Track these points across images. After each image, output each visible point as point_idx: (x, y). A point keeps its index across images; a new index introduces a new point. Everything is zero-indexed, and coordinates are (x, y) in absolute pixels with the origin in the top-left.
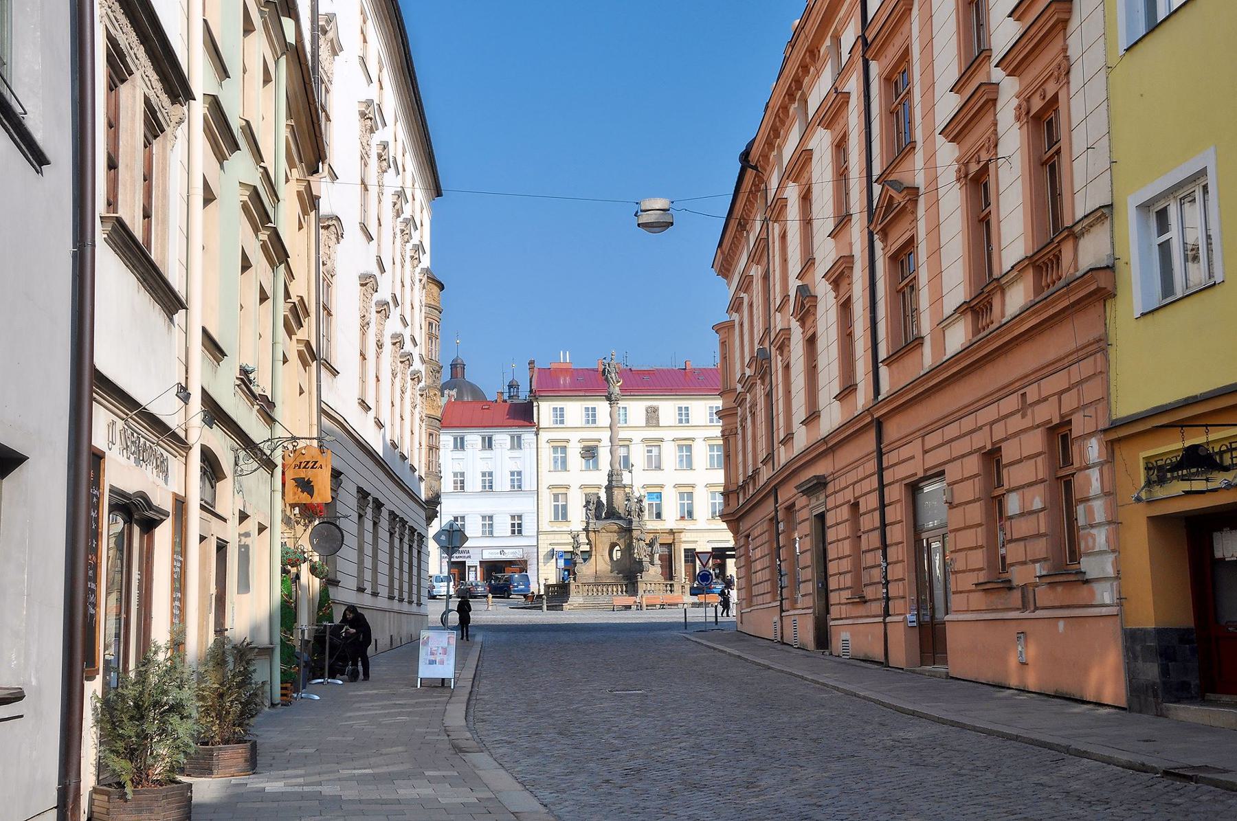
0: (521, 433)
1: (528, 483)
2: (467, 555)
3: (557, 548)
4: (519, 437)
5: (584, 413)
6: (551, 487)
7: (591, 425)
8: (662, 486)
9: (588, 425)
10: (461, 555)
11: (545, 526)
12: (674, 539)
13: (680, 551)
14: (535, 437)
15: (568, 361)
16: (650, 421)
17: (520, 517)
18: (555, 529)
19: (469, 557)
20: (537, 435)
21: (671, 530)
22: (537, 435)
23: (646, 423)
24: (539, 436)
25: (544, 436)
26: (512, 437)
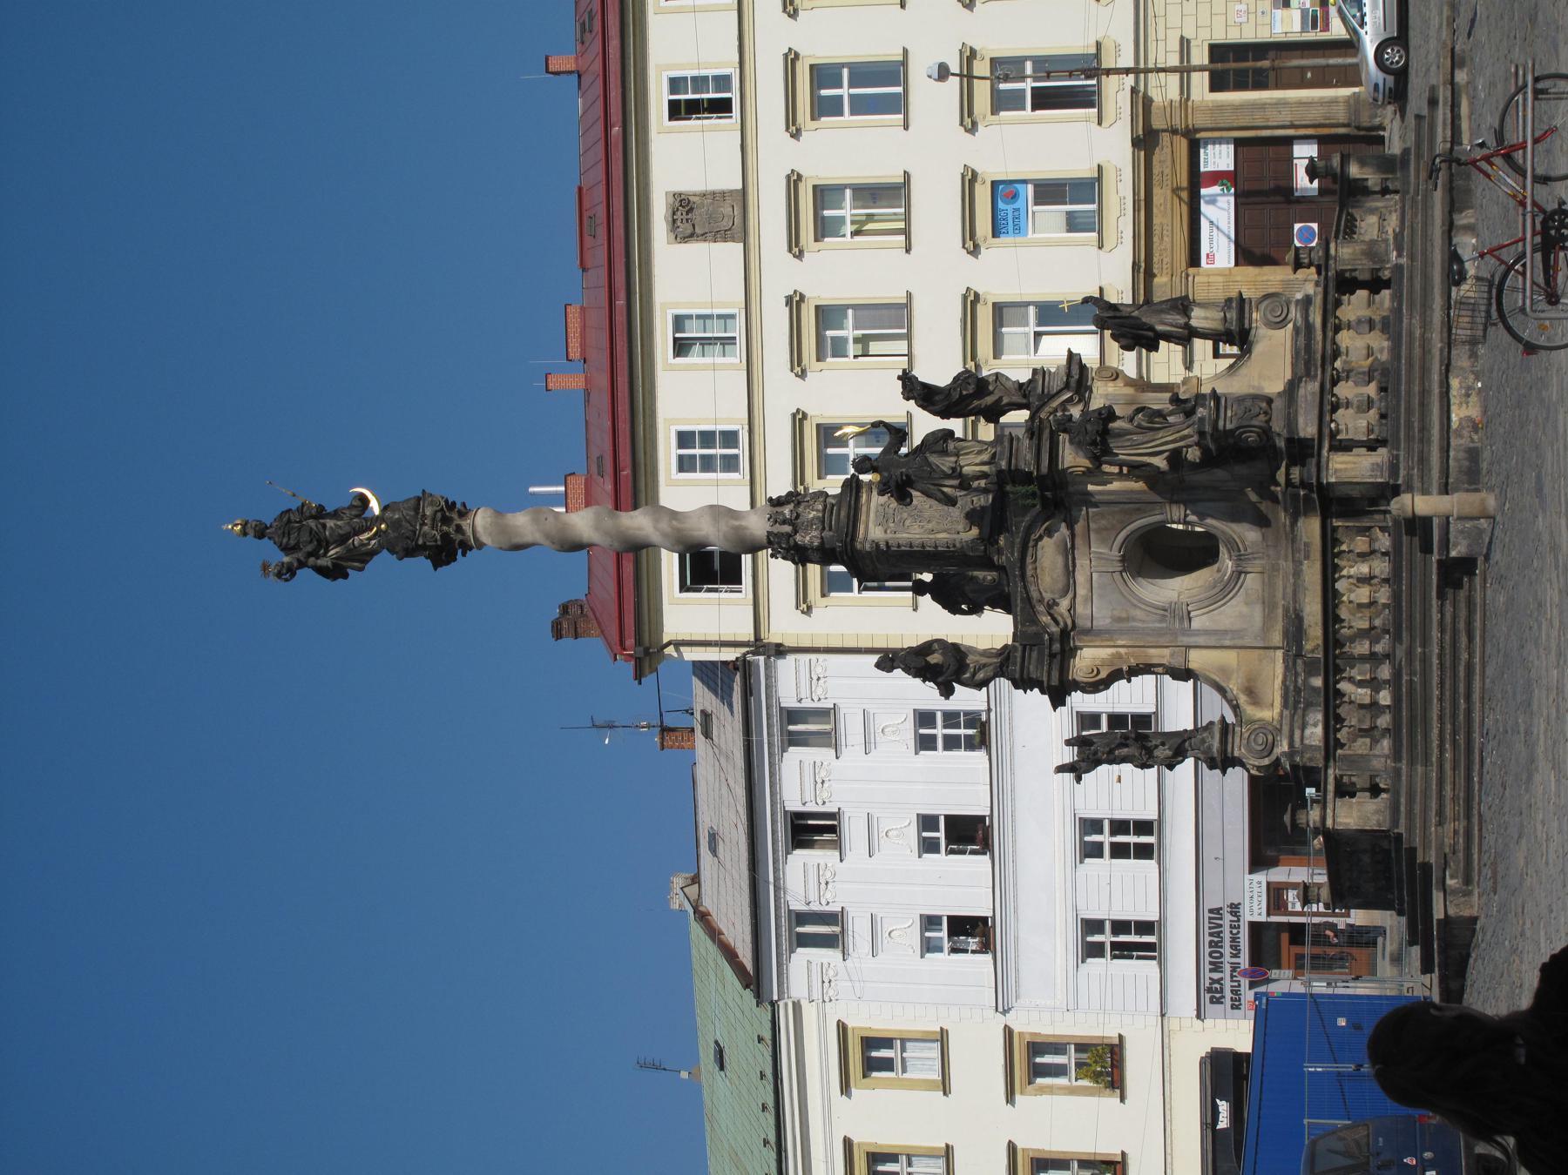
0: (775, 711)
2: (1228, 918)
4: (792, 716)
5: (699, 476)
7: (742, 451)
8: (970, 180)
9: (744, 463)
10: (1227, 936)
12: (1174, 132)
13: (1220, 108)
14: (791, 658)
16: (726, 224)
19: (1235, 909)
20: (780, 651)
21: (1136, 143)
22: (780, 651)
24: (789, 643)
25: (785, 624)
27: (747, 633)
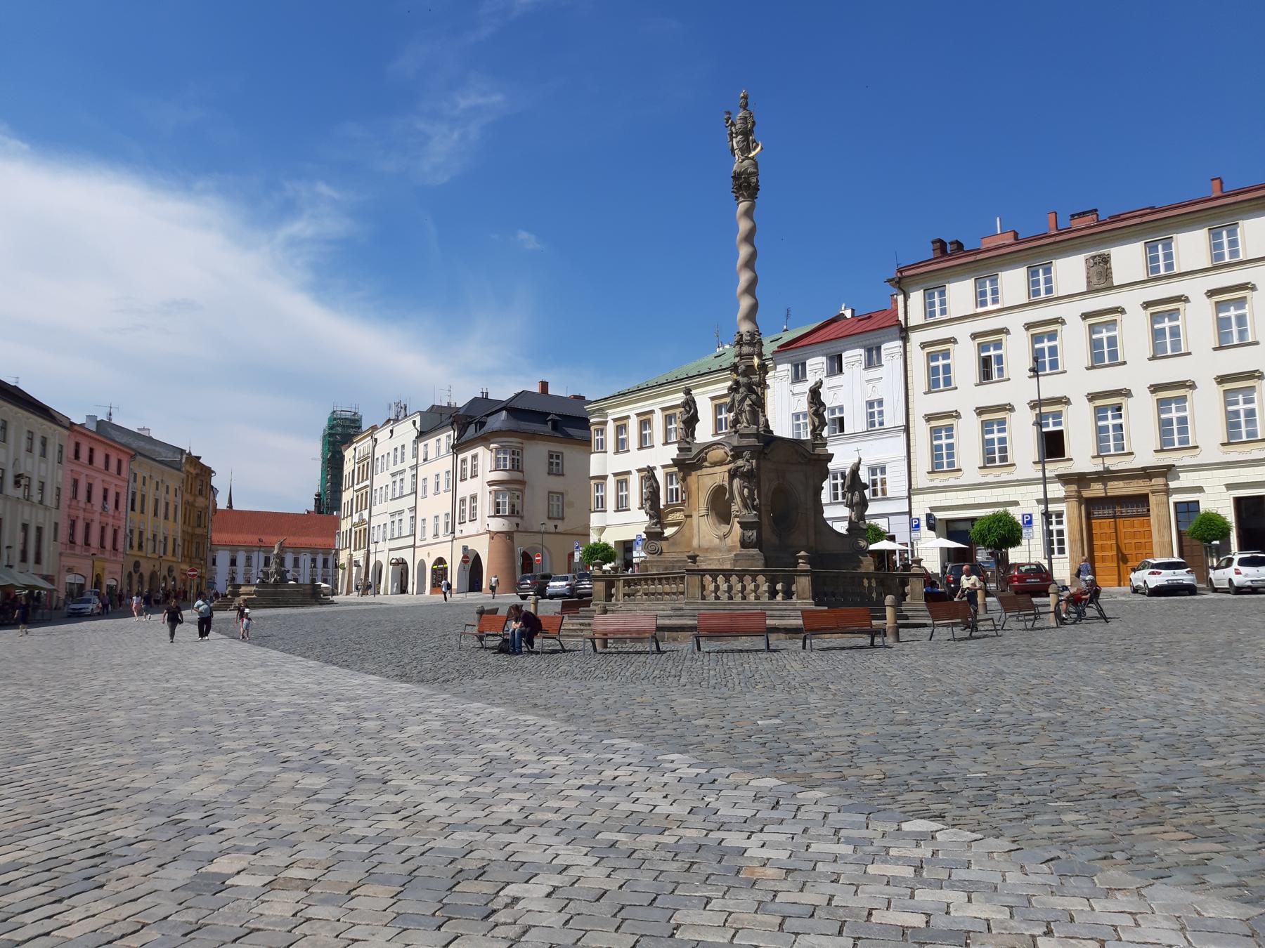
1: (893, 416)
3: (939, 515)
6: (929, 418)
11: (921, 480)
15: (999, 232)
17: (883, 470)
18: (937, 483)
20: (905, 339)
23: (1088, 286)
25: (916, 338)
26: (869, 351)
27: (911, 323)
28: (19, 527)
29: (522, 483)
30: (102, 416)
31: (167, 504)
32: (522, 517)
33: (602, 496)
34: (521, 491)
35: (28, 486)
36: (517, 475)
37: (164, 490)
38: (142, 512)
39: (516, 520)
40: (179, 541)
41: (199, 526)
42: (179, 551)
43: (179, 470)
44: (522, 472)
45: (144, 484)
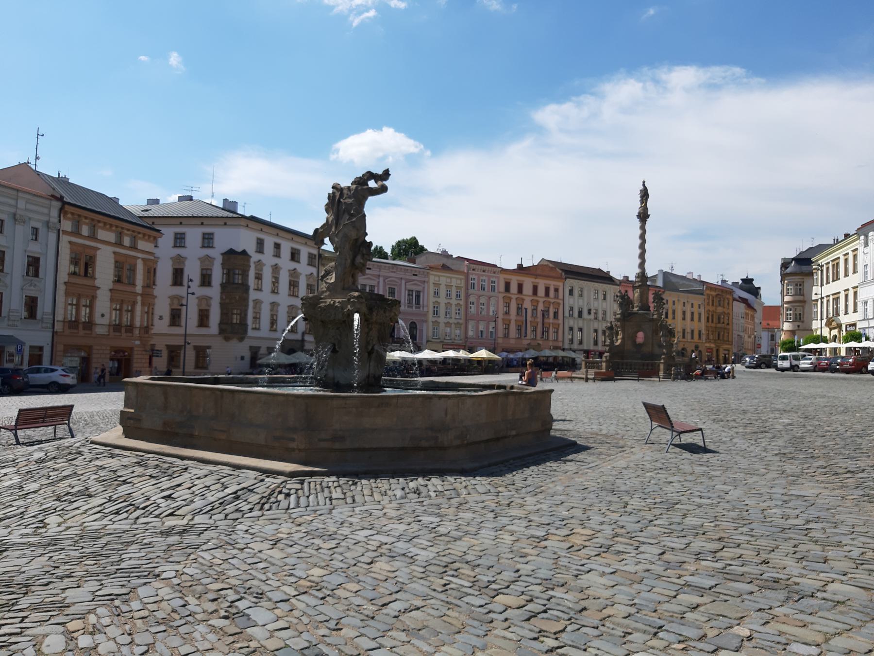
28: (592, 331)
29: (804, 302)
30: (667, 269)
31: (692, 314)
32: (803, 322)
33: (800, 314)
34: (803, 306)
35: (596, 313)
36: (800, 298)
37: (690, 306)
38: (674, 318)
39: (798, 323)
40: (703, 332)
41: (719, 322)
42: (704, 337)
43: (702, 294)
44: (803, 295)
45: (674, 304)
